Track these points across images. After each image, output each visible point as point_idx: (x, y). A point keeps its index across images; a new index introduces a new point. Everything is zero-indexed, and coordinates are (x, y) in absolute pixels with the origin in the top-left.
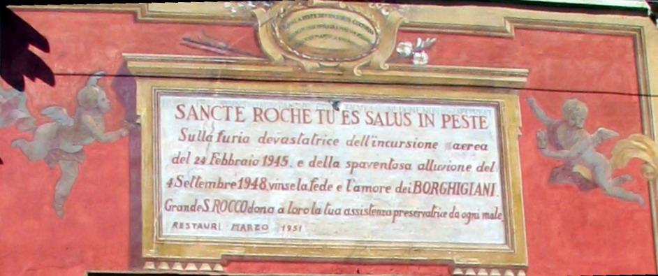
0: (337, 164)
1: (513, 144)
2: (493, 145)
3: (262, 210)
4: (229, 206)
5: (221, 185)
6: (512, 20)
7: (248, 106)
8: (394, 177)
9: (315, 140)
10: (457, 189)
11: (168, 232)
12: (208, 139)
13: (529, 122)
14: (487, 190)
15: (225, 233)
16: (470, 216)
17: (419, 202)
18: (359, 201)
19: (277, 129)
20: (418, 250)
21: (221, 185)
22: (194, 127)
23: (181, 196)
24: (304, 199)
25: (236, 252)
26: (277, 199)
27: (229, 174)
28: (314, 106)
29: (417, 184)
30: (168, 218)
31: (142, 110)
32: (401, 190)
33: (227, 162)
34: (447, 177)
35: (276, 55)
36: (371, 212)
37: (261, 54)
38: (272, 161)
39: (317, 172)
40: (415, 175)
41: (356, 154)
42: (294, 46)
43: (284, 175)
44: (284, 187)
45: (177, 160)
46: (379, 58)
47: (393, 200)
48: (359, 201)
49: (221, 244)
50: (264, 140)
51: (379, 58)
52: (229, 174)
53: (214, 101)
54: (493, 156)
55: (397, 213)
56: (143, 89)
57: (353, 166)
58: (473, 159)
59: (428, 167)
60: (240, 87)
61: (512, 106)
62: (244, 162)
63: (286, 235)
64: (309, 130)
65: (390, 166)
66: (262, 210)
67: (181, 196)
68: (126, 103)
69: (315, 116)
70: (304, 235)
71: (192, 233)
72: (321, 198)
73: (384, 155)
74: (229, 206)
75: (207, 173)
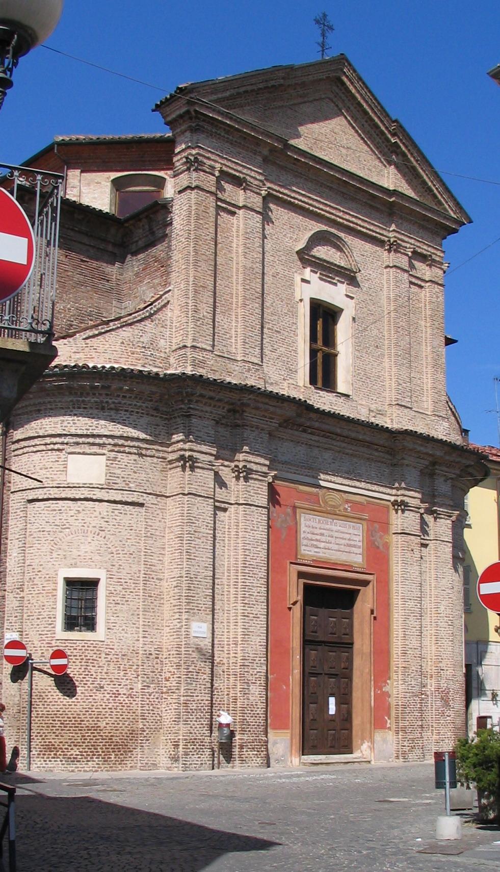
0: (333, 537)
1: (365, 535)
2: (361, 534)
4: (313, 546)
5: (312, 540)
6: (367, 501)
8: (343, 542)
10: (354, 546)
11: (303, 552)
12: (310, 527)
14: (359, 547)
17: (347, 549)
18: (336, 547)
19: (323, 526)
20: (347, 562)
22: (308, 523)
23: (305, 542)
25: (315, 558)
26: (322, 545)
27: (315, 537)
29: (347, 544)
30: (303, 548)
31: (298, 518)
32: (344, 545)
34: (352, 543)
35: (323, 505)
37: (320, 504)
38: (322, 534)
40: (347, 542)
41: (336, 534)
42: (326, 502)
43: (323, 538)
44: (324, 542)
45: (304, 532)
46: (341, 508)
48: (336, 547)
50: (320, 529)
51: (341, 508)
52: (315, 537)
55: (343, 551)
56: (298, 510)
58: (357, 538)
60: (316, 513)
62: (316, 534)
63: (324, 555)
66: (320, 548)
67: (305, 542)
68: (295, 513)
69: (329, 523)
73: (341, 535)
74: (313, 546)
75: (310, 536)
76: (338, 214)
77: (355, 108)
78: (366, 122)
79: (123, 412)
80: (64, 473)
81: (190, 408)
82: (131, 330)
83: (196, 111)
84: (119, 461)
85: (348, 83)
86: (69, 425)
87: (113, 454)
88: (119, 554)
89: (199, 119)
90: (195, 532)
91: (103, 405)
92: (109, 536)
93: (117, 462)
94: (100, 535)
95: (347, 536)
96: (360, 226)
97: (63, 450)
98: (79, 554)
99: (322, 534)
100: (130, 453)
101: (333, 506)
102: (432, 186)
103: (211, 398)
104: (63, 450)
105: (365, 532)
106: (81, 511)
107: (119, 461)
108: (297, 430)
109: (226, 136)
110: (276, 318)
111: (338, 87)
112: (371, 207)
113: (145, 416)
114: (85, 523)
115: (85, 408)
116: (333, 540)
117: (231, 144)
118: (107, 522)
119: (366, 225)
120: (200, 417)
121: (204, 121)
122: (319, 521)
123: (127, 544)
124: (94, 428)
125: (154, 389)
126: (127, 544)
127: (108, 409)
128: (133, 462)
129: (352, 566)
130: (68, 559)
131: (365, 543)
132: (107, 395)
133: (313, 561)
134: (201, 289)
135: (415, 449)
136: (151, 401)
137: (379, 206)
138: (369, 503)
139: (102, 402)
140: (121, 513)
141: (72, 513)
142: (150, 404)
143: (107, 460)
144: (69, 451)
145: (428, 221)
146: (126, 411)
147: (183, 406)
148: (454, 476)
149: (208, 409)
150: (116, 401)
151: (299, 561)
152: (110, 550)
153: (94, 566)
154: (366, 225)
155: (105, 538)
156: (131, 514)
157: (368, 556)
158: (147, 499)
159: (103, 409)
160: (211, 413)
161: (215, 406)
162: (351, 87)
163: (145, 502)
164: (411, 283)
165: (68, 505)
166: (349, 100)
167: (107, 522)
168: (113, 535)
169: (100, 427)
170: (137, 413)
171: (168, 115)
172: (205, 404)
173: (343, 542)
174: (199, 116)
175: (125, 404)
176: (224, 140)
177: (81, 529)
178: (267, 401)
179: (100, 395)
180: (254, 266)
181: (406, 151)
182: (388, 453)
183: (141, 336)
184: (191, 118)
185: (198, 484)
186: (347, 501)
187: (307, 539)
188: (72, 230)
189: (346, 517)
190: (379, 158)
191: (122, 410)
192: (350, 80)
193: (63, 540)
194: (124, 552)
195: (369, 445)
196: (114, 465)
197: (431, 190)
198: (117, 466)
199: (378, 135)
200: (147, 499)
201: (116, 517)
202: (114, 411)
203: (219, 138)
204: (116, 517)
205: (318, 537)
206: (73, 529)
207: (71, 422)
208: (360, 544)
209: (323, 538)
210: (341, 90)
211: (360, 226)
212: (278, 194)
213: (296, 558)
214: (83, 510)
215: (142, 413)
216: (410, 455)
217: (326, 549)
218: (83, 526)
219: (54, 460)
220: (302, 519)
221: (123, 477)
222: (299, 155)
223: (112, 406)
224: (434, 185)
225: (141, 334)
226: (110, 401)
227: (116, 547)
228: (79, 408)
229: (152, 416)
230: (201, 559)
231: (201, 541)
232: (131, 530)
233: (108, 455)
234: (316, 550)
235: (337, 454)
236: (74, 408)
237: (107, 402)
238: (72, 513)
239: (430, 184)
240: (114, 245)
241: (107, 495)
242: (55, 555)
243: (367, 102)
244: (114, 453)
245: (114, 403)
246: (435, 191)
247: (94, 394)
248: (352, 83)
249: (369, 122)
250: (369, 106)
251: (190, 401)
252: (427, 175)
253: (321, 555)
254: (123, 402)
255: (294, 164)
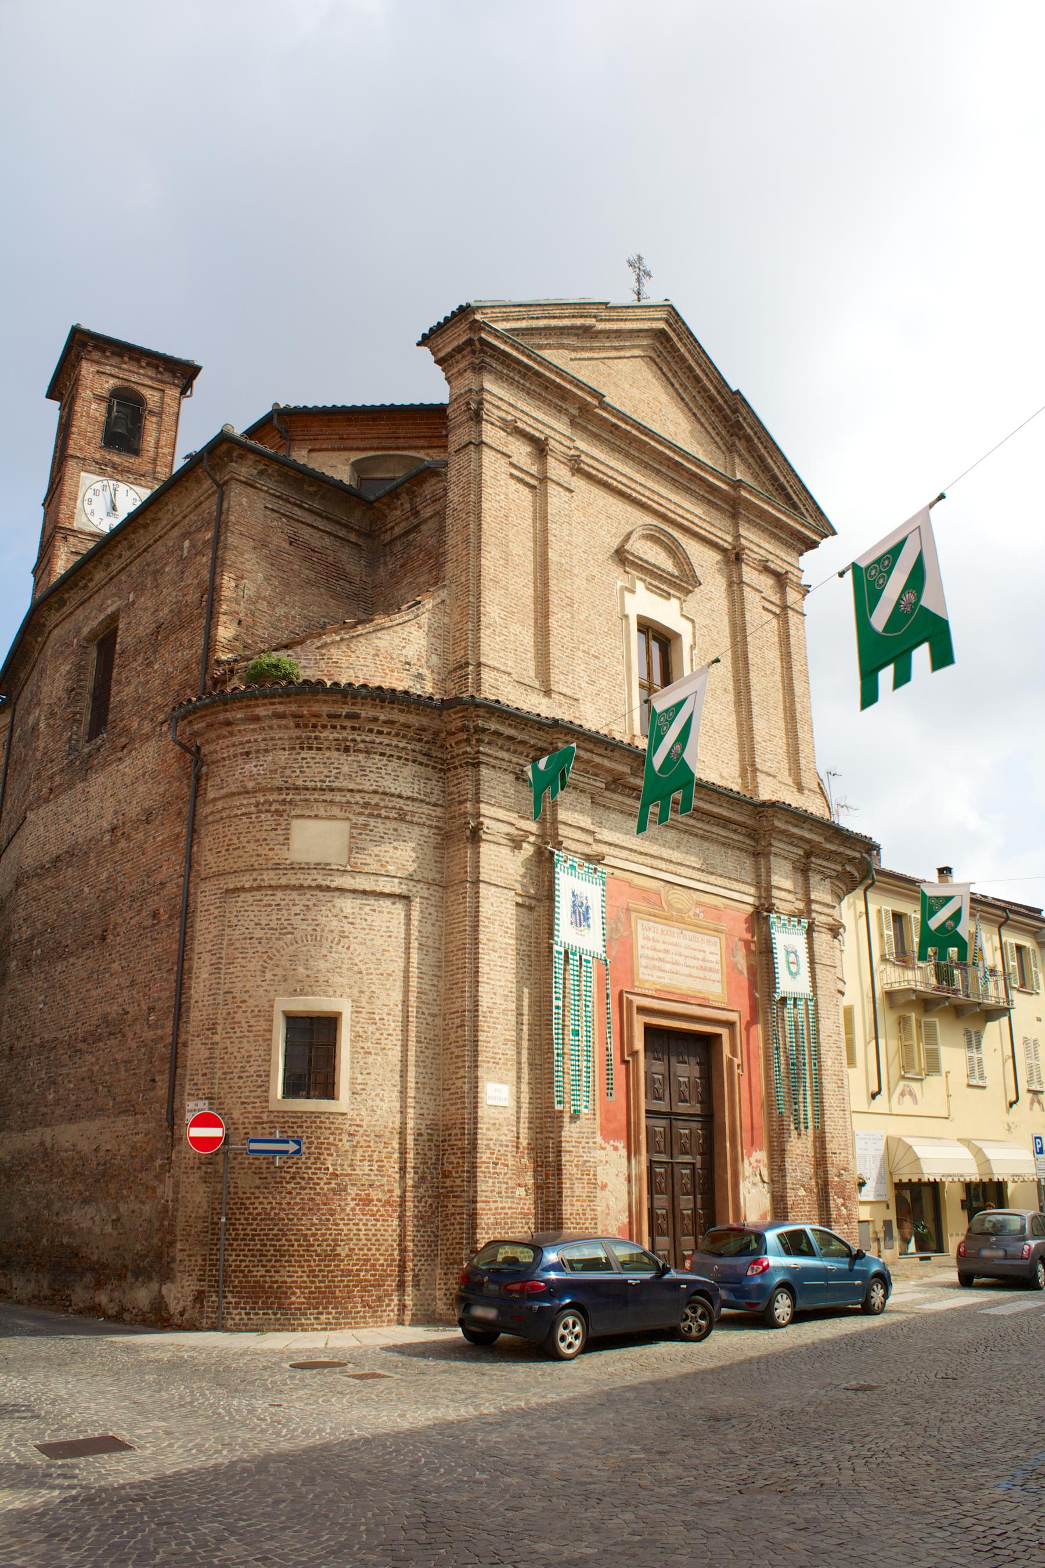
3: (664, 971)
4: (654, 967)
5: (654, 959)
7: (660, 927)
8: (695, 963)
9: (676, 945)
10: (711, 970)
11: (641, 976)
13: (727, 946)
14: (717, 971)
15: (654, 979)
16: (714, 981)
17: (701, 974)
18: (686, 971)
19: (667, 939)
21: (654, 959)
22: (647, 933)
24: (675, 968)
25: (658, 987)
26: (668, 967)
27: (656, 955)
28: (677, 930)
30: (642, 970)
33: (655, 950)
34: (708, 965)
36: (691, 976)
38: (667, 951)
39: (677, 958)
40: (701, 963)
42: (670, 905)
43: (668, 957)
44: (669, 963)
46: (691, 914)
47: (695, 972)
48: (686, 971)
49: (654, 983)
50: (664, 942)
51: (691, 914)
53: (651, 924)
54: (718, 958)
56: (633, 915)
57: (686, 957)
58: (713, 958)
59: (704, 960)
60: (657, 919)
61: (723, 936)
62: (660, 951)
64: (674, 940)
65: (695, 958)
66: (664, 971)
68: (629, 920)
70: (674, 982)
71: (647, 977)
72: (678, 968)
74: (654, 967)
75: (650, 953)
76: (668, 506)
77: (685, 373)
78: (699, 392)
79: (377, 757)
80: (285, 847)
81: (478, 752)
82: (388, 637)
83: (481, 340)
84: (372, 831)
85: (675, 339)
86: (294, 775)
87: (361, 820)
88: (371, 974)
89: (485, 353)
90: (488, 940)
91: (348, 744)
92: (357, 947)
93: (368, 832)
94: (342, 944)
95: (700, 955)
96: (697, 525)
97: (285, 811)
98: (308, 972)
99: (667, 951)
100: (387, 818)
101: (680, 911)
102: (786, 483)
103: (510, 738)
104: (285, 811)
105: (724, 950)
106: (311, 906)
107: (372, 831)
108: (629, 796)
109: (522, 381)
110: (593, 637)
111: (662, 343)
112: (710, 502)
113: (410, 763)
114: (317, 925)
115: (319, 749)
116: (681, 960)
117: (528, 393)
118: (352, 923)
119: (704, 525)
120: (494, 767)
121: (492, 356)
122: (662, 931)
123: (383, 958)
124: (332, 779)
125: (425, 721)
126: (383, 958)
127: (354, 751)
128: (392, 832)
129: (708, 1000)
130: (289, 981)
131: (724, 965)
132: (353, 728)
133: (656, 990)
134: (491, 584)
135: (788, 831)
136: (420, 740)
137: (719, 503)
138: (726, 907)
139: (345, 740)
140: (374, 911)
141: (297, 909)
142: (418, 747)
143: (352, 828)
144: (293, 813)
145: (781, 528)
146: (382, 754)
147: (468, 749)
148: (834, 874)
149: (505, 755)
150: (367, 739)
151: (636, 990)
152: (356, 968)
153: (331, 993)
154: (704, 525)
155: (348, 948)
156: (389, 913)
157: (729, 983)
158: (414, 889)
159: (347, 750)
160: (510, 762)
161: (515, 752)
162: (679, 345)
163: (410, 894)
164: (764, 608)
165: (291, 897)
166: (676, 362)
167: (352, 923)
168: (361, 944)
169: (342, 777)
170: (399, 758)
171: (439, 350)
172: (501, 748)
173: (695, 963)
174: (485, 348)
175: (381, 743)
176: (518, 387)
177: (311, 935)
178: (590, 746)
179: (344, 728)
180: (563, 561)
181: (752, 434)
182: (749, 836)
183: (404, 647)
184: (474, 352)
185: (493, 867)
186: (699, 904)
187: (647, 957)
188: (300, 507)
189: (697, 927)
190: (716, 442)
191: (375, 753)
192: (678, 335)
193: (282, 952)
194: (379, 972)
195: (725, 822)
196: (364, 836)
197: (784, 489)
198: (368, 838)
199: (713, 411)
200: (414, 889)
201: (367, 917)
202: (364, 755)
203: (512, 384)
204: (367, 917)
205: (662, 955)
206: (298, 934)
207: (298, 771)
208: (718, 967)
209: (668, 957)
210: (665, 347)
211: (697, 525)
212: (591, 470)
213: (633, 986)
214: (315, 905)
215: (406, 759)
216: (780, 840)
217: (672, 973)
218: (315, 930)
219: (269, 828)
220: (639, 927)
221: (376, 855)
222: (619, 419)
223: (362, 746)
224: (788, 482)
225: (403, 644)
226: (358, 738)
227: (366, 963)
228: (311, 748)
229: (421, 764)
230: (498, 983)
231: (497, 955)
232: (390, 936)
233: (354, 821)
234: (660, 974)
235: (682, 836)
236: (302, 748)
237: (354, 740)
238: (297, 909)
239: (782, 479)
240: (359, 533)
241: (352, 881)
242: (268, 976)
243: (700, 366)
244: (363, 818)
245: (363, 741)
246: (789, 490)
247: (334, 727)
248: (681, 340)
249: (703, 393)
250: (703, 371)
251: (479, 741)
252: (778, 467)
253: (666, 981)
254: (378, 740)
255: (611, 432)
